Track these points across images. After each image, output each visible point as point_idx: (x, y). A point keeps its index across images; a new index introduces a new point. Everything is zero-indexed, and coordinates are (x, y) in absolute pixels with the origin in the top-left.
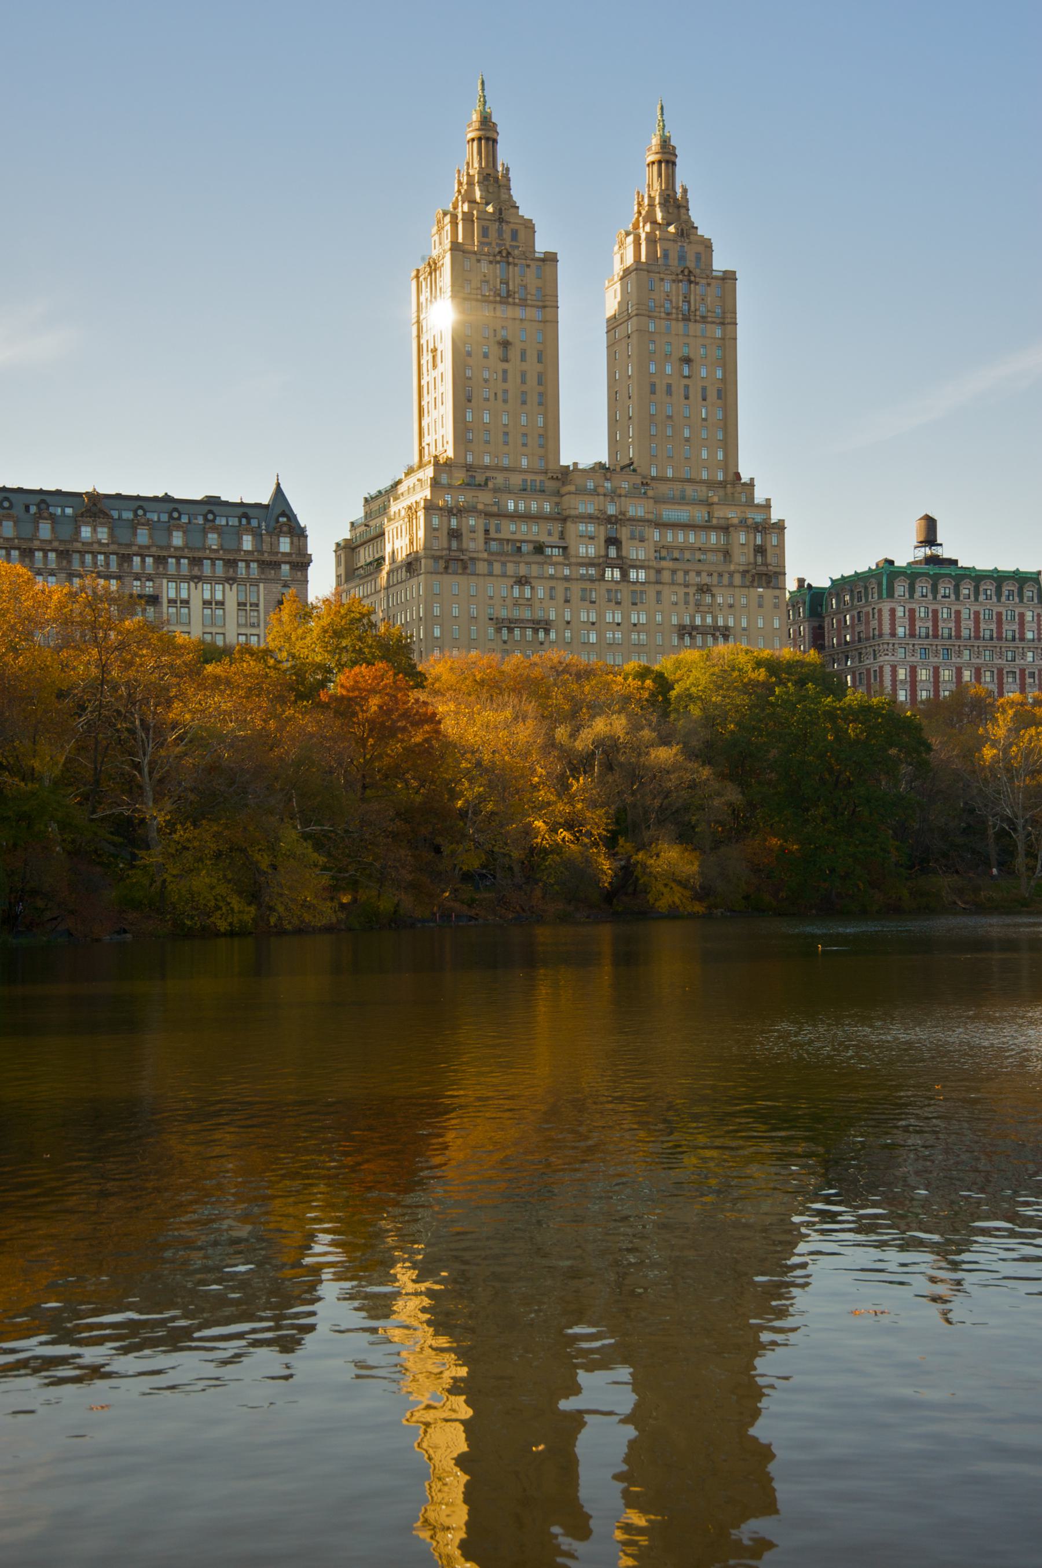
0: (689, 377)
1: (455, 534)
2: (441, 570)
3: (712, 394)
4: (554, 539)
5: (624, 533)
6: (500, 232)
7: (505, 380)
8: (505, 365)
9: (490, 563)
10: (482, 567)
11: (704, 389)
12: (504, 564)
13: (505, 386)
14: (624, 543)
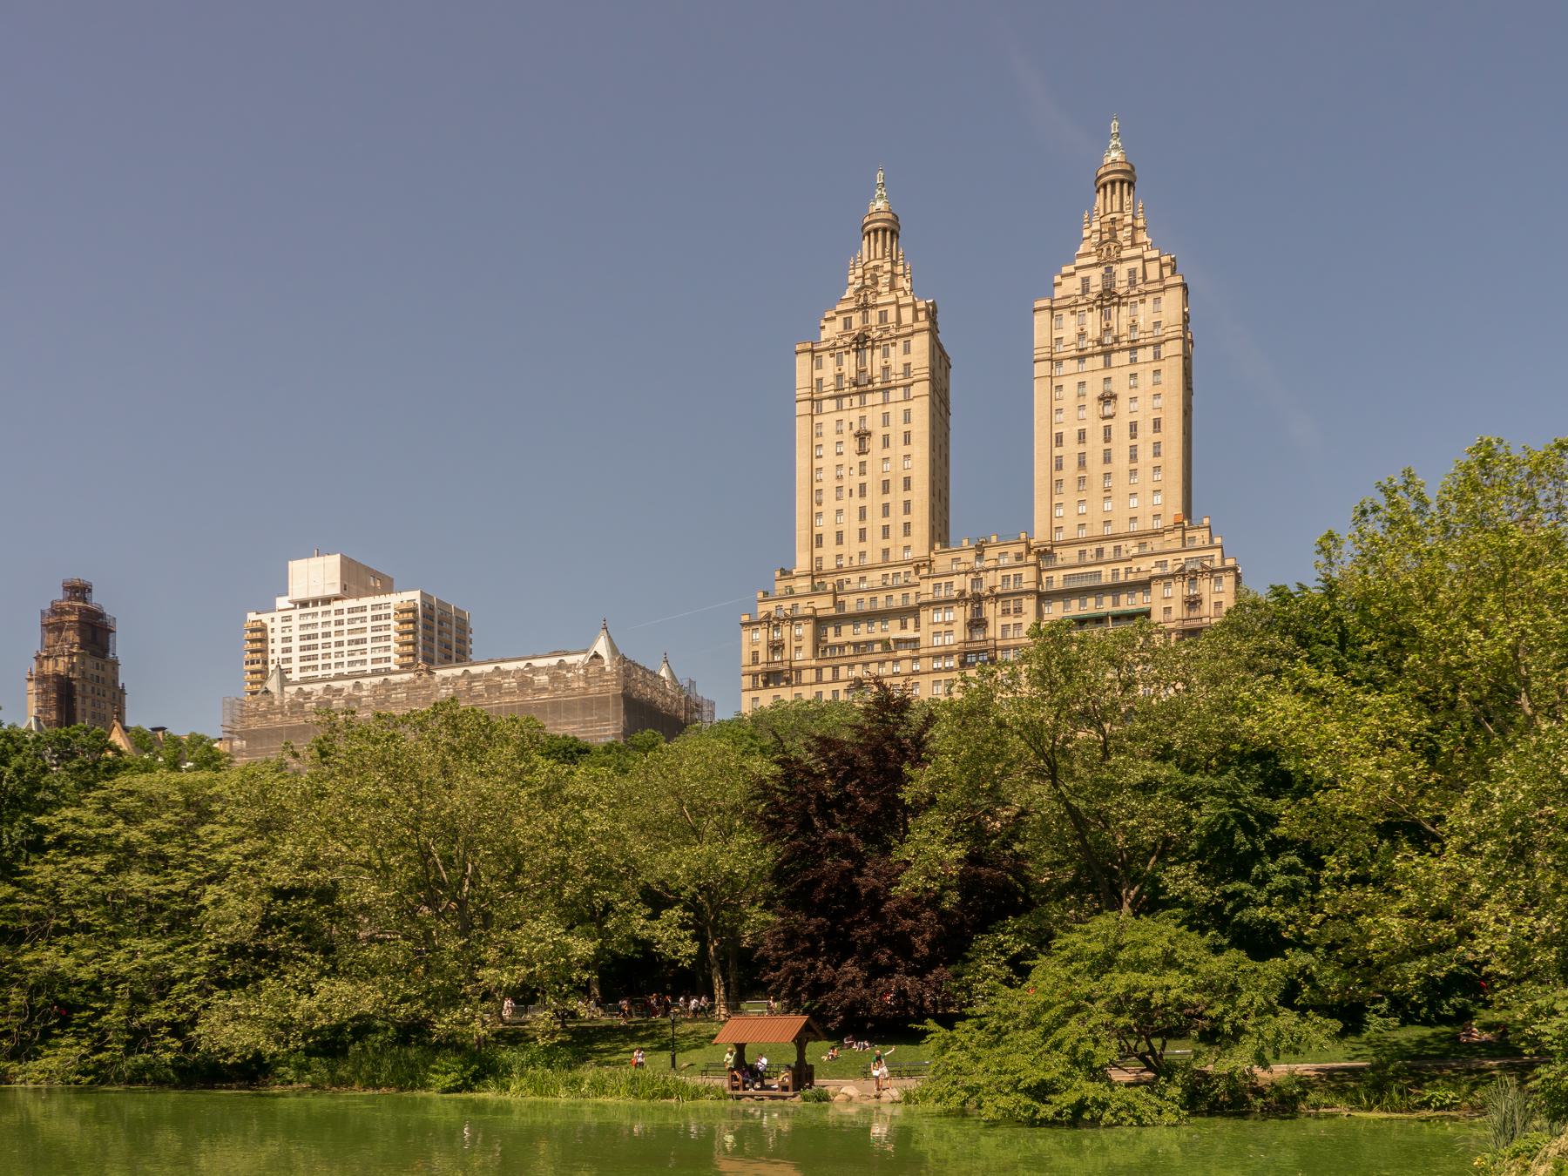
0: (1111, 417)
1: (776, 647)
2: (761, 684)
3: (1145, 430)
4: (909, 633)
5: (990, 611)
6: (865, 319)
7: (863, 473)
8: (863, 458)
9: (819, 670)
10: (809, 676)
11: (1133, 426)
12: (836, 668)
13: (863, 479)
14: (991, 623)
